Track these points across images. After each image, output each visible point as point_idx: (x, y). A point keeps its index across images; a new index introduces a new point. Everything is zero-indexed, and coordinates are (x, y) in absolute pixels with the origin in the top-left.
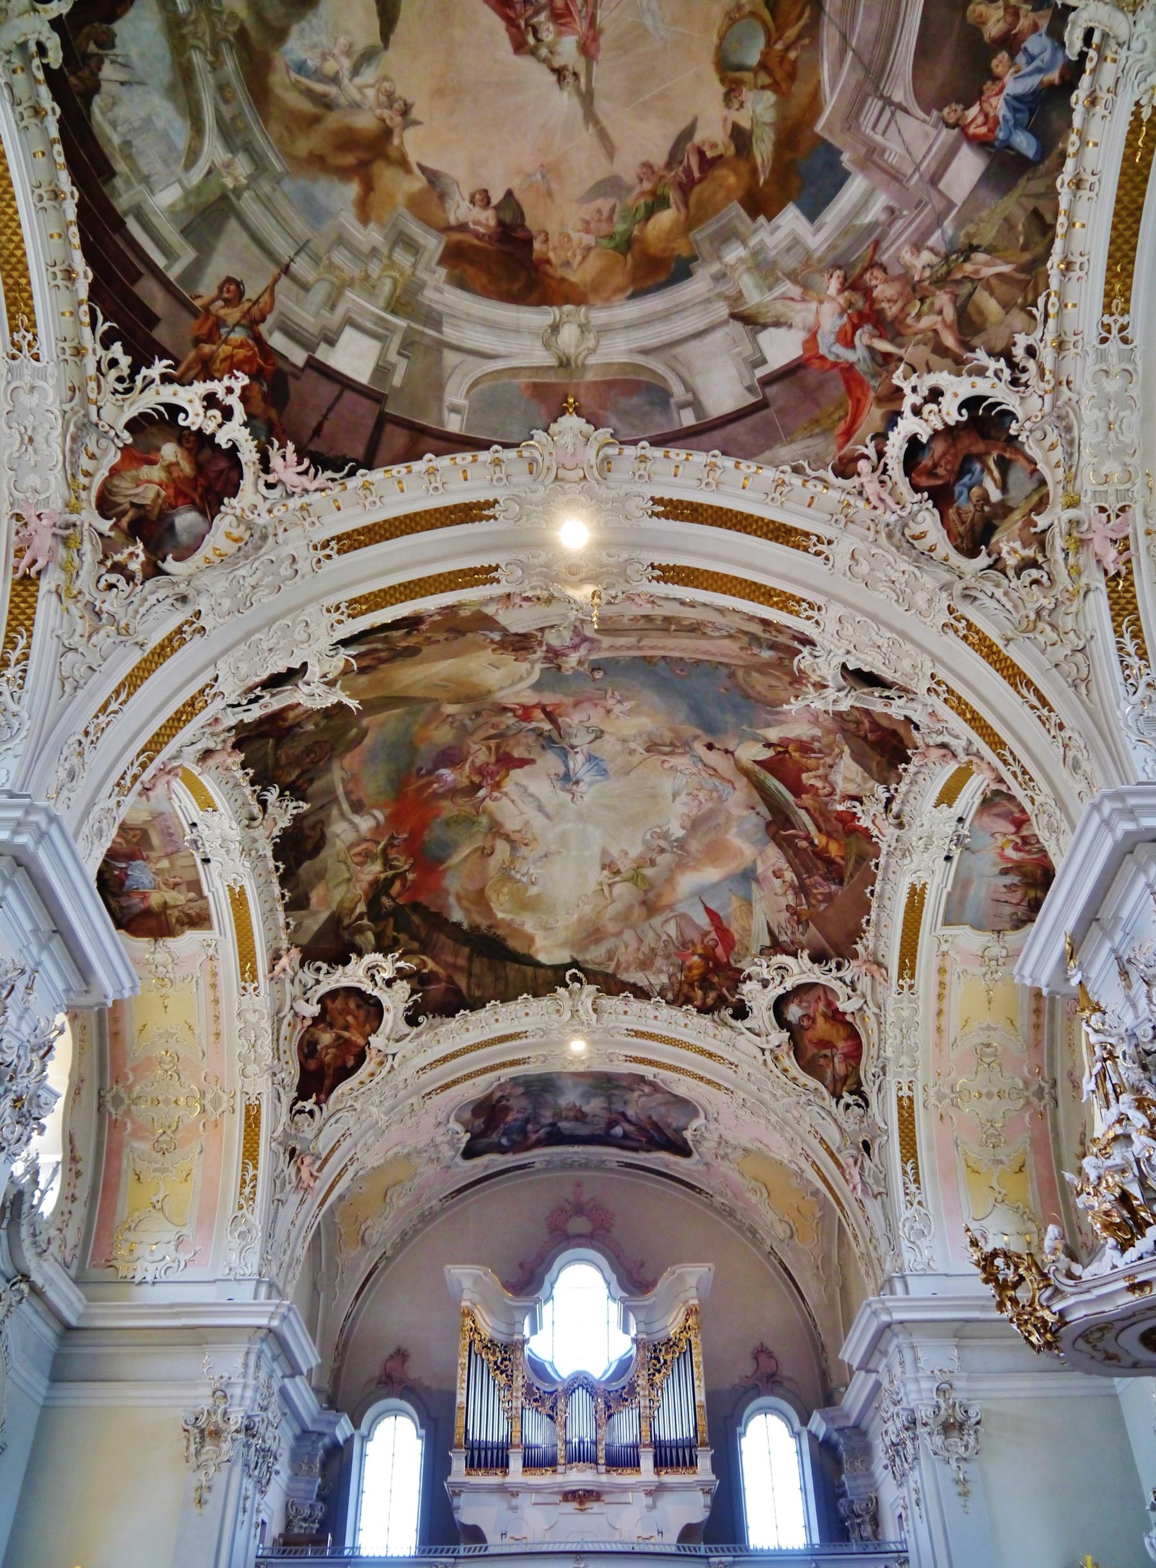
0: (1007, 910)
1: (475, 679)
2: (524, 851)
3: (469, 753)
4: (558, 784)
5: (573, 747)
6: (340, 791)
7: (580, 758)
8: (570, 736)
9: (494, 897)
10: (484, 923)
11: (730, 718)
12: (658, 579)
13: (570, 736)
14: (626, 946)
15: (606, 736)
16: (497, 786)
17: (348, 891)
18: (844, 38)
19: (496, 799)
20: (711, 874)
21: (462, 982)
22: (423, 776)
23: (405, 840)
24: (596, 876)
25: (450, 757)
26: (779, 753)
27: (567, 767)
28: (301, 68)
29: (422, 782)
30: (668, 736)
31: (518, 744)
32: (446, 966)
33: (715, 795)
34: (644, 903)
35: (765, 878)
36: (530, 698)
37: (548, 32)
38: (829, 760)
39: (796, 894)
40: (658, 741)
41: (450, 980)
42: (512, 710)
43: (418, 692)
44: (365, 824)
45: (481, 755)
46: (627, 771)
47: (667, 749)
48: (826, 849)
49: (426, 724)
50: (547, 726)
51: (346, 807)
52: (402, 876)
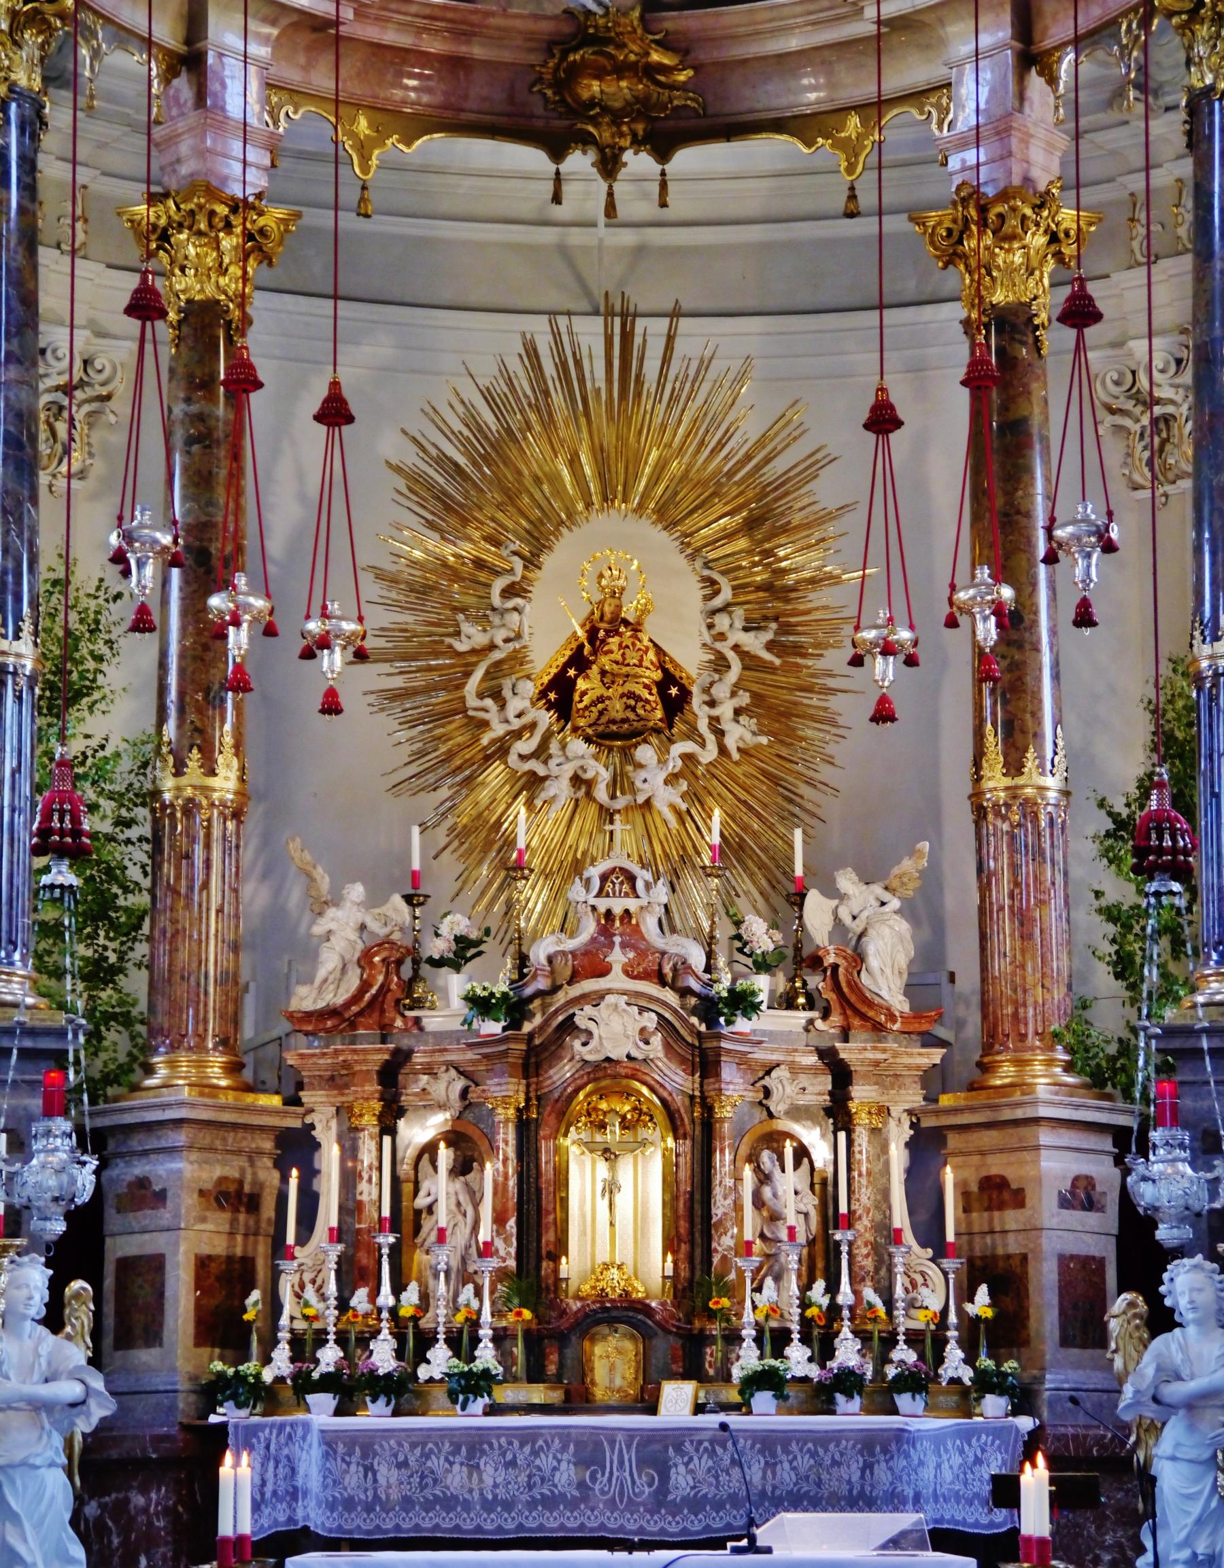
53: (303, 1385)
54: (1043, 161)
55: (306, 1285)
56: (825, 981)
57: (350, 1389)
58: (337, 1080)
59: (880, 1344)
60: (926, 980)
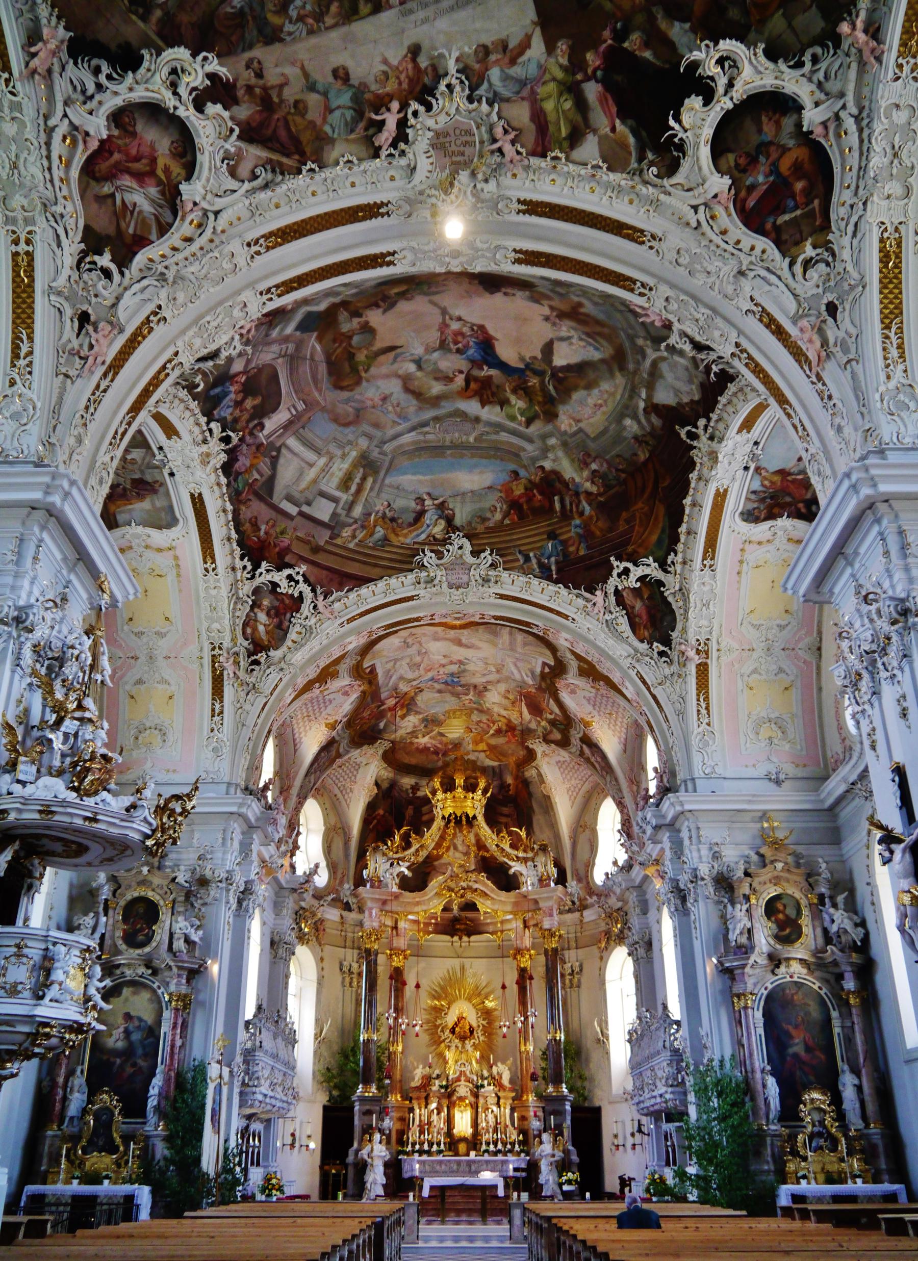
12: (383, 204)
18: (312, 359)
28: (596, 349)
37: (466, 330)
53: (413, 1152)
54: (527, 942)
55: (413, 1135)
56: (496, 1081)
57: (421, 1152)
58: (418, 1099)
59: (505, 1144)
60: (511, 1081)
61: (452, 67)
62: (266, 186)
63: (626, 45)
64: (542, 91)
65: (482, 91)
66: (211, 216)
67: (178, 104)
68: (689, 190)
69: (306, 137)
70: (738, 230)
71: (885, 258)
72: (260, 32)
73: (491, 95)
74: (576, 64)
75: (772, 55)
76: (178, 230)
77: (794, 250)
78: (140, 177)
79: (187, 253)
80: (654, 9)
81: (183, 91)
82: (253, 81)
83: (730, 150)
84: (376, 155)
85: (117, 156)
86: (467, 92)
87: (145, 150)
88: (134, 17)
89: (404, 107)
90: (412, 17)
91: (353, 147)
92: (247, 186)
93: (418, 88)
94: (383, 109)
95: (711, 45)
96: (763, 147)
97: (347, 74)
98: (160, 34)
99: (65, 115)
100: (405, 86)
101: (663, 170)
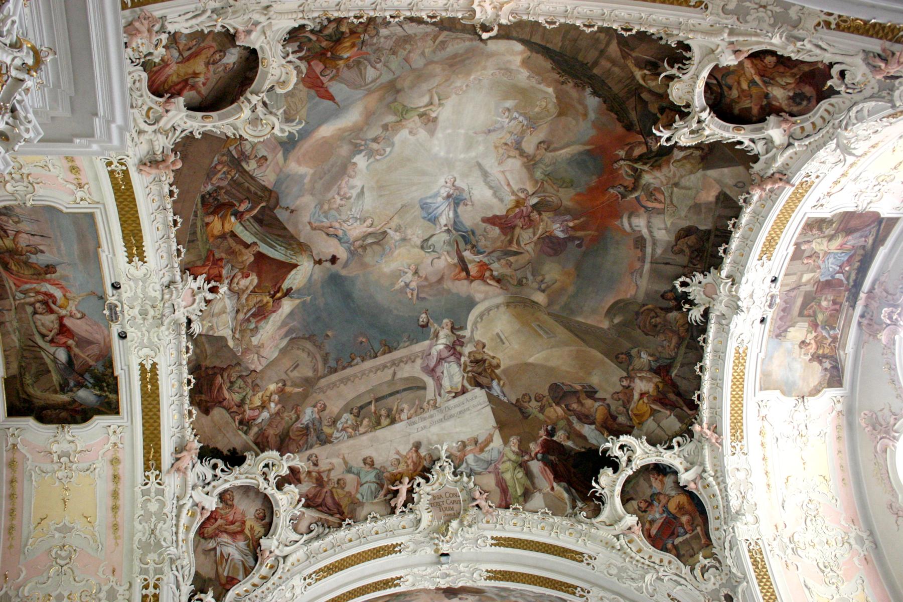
0: (25, 226)
1: (517, 326)
2: (509, 139)
3: (536, 244)
4: (465, 195)
5: (448, 231)
6: (647, 266)
7: (443, 220)
8: (449, 243)
9: (550, 106)
10: (569, 87)
11: (321, 302)
13: (449, 243)
14: (423, 54)
15: (419, 242)
16: (518, 203)
17: (682, 177)
19: (523, 190)
20: (326, 131)
21: (614, 49)
22: (578, 238)
23: (613, 187)
24: (444, 113)
25: (552, 246)
26: (278, 291)
27: (455, 212)
29: (580, 234)
30: (368, 259)
31: (494, 241)
32: (624, 67)
33: (326, 207)
34: (398, 91)
35: (274, 150)
36: (478, 290)
38: (241, 316)
39: (242, 153)
40: (375, 247)
41: (625, 56)
42: (493, 277)
43: (562, 333)
44: (640, 223)
45: (527, 238)
46: (404, 209)
47: (369, 241)
48: (223, 219)
49: (563, 289)
50: (467, 254)
51: (649, 250)
52: (628, 158)
61: (443, 455)
62: (318, 537)
63: (555, 438)
64: (502, 467)
65: (462, 468)
66: (281, 561)
67: (266, 486)
68: (610, 525)
69: (344, 503)
70: (649, 549)
71: (755, 563)
72: (318, 438)
73: (468, 471)
74: (523, 450)
75: (652, 443)
76: (258, 571)
77: (690, 560)
78: (233, 535)
79: (264, 588)
80: (571, 418)
81: (271, 477)
82: (312, 468)
83: (632, 499)
84: (393, 511)
85: (220, 521)
86: (453, 469)
87: (238, 517)
88: (240, 432)
89: (412, 479)
90: (416, 426)
91: (377, 508)
92: (305, 537)
93: (420, 469)
94: (397, 482)
95: (615, 438)
96: (655, 496)
97: (373, 461)
98: (257, 444)
99: (191, 497)
100: (411, 467)
101: (590, 513)
